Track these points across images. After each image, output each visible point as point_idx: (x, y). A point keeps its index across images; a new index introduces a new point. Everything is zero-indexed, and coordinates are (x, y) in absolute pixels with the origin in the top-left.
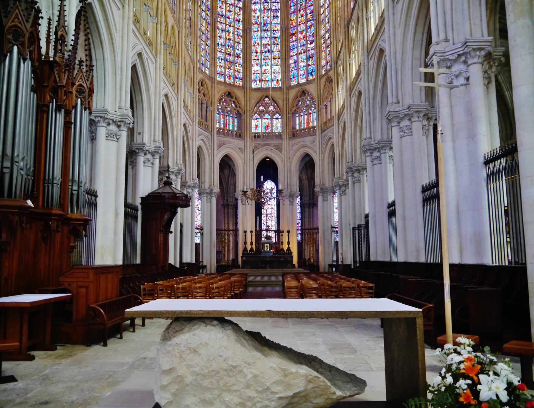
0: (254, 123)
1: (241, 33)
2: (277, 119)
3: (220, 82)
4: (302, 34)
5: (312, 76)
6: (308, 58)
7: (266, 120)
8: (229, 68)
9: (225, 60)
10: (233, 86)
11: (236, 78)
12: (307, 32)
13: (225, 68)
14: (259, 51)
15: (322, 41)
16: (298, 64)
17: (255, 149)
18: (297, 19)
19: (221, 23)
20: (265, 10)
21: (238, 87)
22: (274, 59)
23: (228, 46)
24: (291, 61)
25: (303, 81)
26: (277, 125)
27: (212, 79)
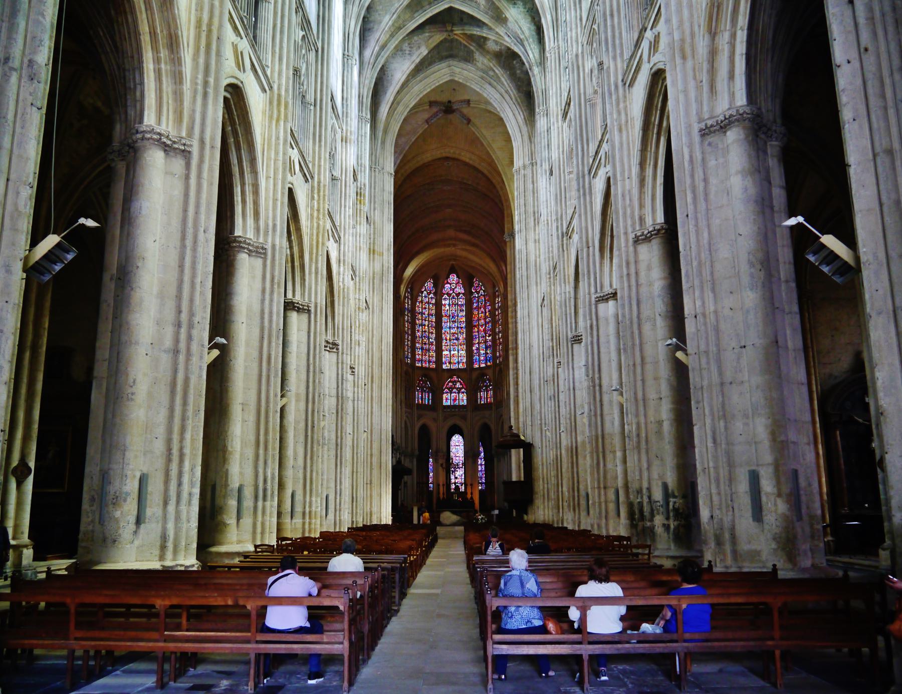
0: (445, 396)
1: (434, 324)
2: (463, 393)
3: (418, 367)
6: (487, 348)
8: (425, 355)
9: (422, 348)
10: (429, 369)
13: (422, 355)
17: (445, 419)
18: (478, 314)
21: (432, 369)
24: (474, 348)
26: (463, 399)
27: (413, 365)
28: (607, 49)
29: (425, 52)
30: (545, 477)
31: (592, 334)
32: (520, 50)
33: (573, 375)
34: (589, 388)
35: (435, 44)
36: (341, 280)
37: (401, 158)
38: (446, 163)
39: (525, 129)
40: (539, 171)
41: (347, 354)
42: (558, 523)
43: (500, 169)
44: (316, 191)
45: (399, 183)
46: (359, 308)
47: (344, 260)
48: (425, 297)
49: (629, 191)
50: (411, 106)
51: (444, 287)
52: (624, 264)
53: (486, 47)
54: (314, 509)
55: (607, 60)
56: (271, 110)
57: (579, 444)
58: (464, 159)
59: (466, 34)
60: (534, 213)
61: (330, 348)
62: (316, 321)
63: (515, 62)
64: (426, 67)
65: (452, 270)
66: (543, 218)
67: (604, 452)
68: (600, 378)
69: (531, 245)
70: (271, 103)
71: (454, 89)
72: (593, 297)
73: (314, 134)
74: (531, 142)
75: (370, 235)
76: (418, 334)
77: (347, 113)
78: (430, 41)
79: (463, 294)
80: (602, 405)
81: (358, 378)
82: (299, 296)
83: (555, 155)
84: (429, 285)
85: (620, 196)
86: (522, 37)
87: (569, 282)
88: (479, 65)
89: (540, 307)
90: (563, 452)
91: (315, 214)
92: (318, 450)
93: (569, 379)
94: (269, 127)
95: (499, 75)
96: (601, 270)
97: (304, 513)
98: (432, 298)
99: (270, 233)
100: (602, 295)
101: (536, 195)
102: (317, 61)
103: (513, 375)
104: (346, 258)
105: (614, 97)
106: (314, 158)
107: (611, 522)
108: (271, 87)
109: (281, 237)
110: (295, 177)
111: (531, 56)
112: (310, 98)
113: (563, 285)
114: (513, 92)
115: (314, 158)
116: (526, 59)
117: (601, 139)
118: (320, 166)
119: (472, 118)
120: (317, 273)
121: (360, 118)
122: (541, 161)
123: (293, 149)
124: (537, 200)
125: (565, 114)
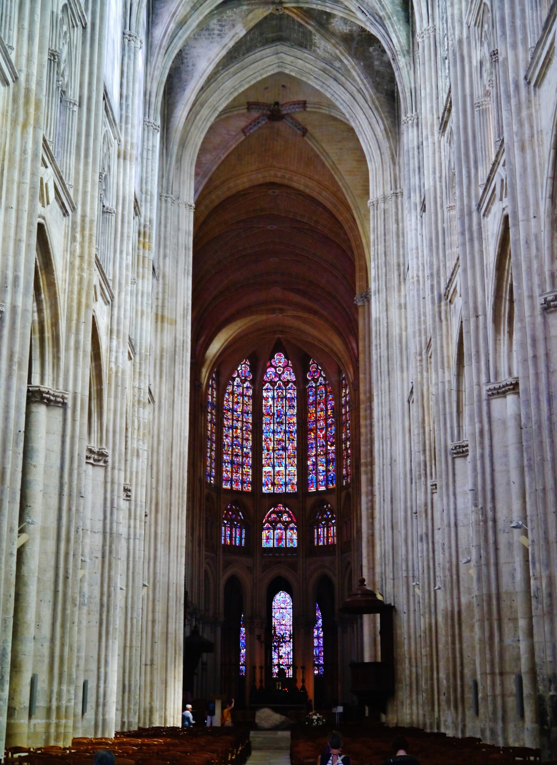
0: (265, 534)
2: (292, 529)
3: (226, 490)
4: (321, 432)
5: (333, 484)
6: (328, 462)
7: (279, 531)
8: (237, 472)
9: (232, 462)
10: (242, 493)
11: (245, 483)
12: (327, 430)
14: (271, 448)
15: (344, 448)
16: (317, 467)
18: (316, 412)
19: (228, 419)
20: (278, 397)
21: (247, 493)
22: (289, 458)
23: (236, 445)
24: (309, 463)
25: (322, 488)
28: (504, 33)
29: (243, 33)
30: (413, 656)
31: (482, 443)
32: (379, 32)
33: (455, 504)
34: (477, 524)
35: (256, 21)
36: (113, 359)
37: (204, 182)
38: (270, 192)
39: (385, 145)
40: (406, 205)
41: (120, 470)
42: (431, 728)
43: (349, 201)
44: (79, 229)
45: (202, 219)
46: (139, 401)
47: (118, 331)
48: (238, 386)
49: (536, 236)
50: (221, 109)
51: (266, 373)
52: (529, 341)
53: (330, 26)
54: (64, 702)
55: (503, 48)
56: (15, 110)
57: (463, 608)
58: (295, 185)
59: (301, 8)
60: (399, 265)
61: (95, 460)
62: (74, 420)
63: (371, 49)
64: (244, 54)
65: (278, 348)
66: (412, 273)
67: (500, 620)
68: (494, 509)
69: (394, 312)
70: (15, 100)
71: (284, 86)
72: (485, 389)
73: (78, 147)
74: (394, 164)
75: (157, 294)
76: (227, 441)
77: (127, 117)
78: (250, 16)
79: (294, 382)
80: (496, 549)
81: (136, 506)
82: (50, 383)
83: (428, 182)
84: (243, 368)
85: (522, 242)
86: (382, 13)
87: (449, 367)
88: (320, 52)
89: (406, 404)
90: (440, 619)
91: (77, 262)
92: (73, 612)
93: (449, 510)
94: (12, 135)
95: (349, 67)
96: (496, 350)
97: (49, 710)
98: (247, 388)
99: (9, 289)
100: (497, 386)
101: (401, 239)
102: (84, 43)
103: (367, 503)
104: (122, 328)
105: (513, 101)
106: (77, 180)
107: (511, 727)
108: (16, 78)
109: (25, 295)
110: (48, 208)
111: (395, 40)
112: (73, 94)
113: (440, 371)
114: (369, 92)
115: (77, 180)
116: (388, 45)
117: (496, 161)
118: (85, 193)
119: (309, 128)
120: (77, 349)
121: (146, 125)
122: (409, 190)
123: (46, 167)
124: (403, 247)
125: (444, 125)
